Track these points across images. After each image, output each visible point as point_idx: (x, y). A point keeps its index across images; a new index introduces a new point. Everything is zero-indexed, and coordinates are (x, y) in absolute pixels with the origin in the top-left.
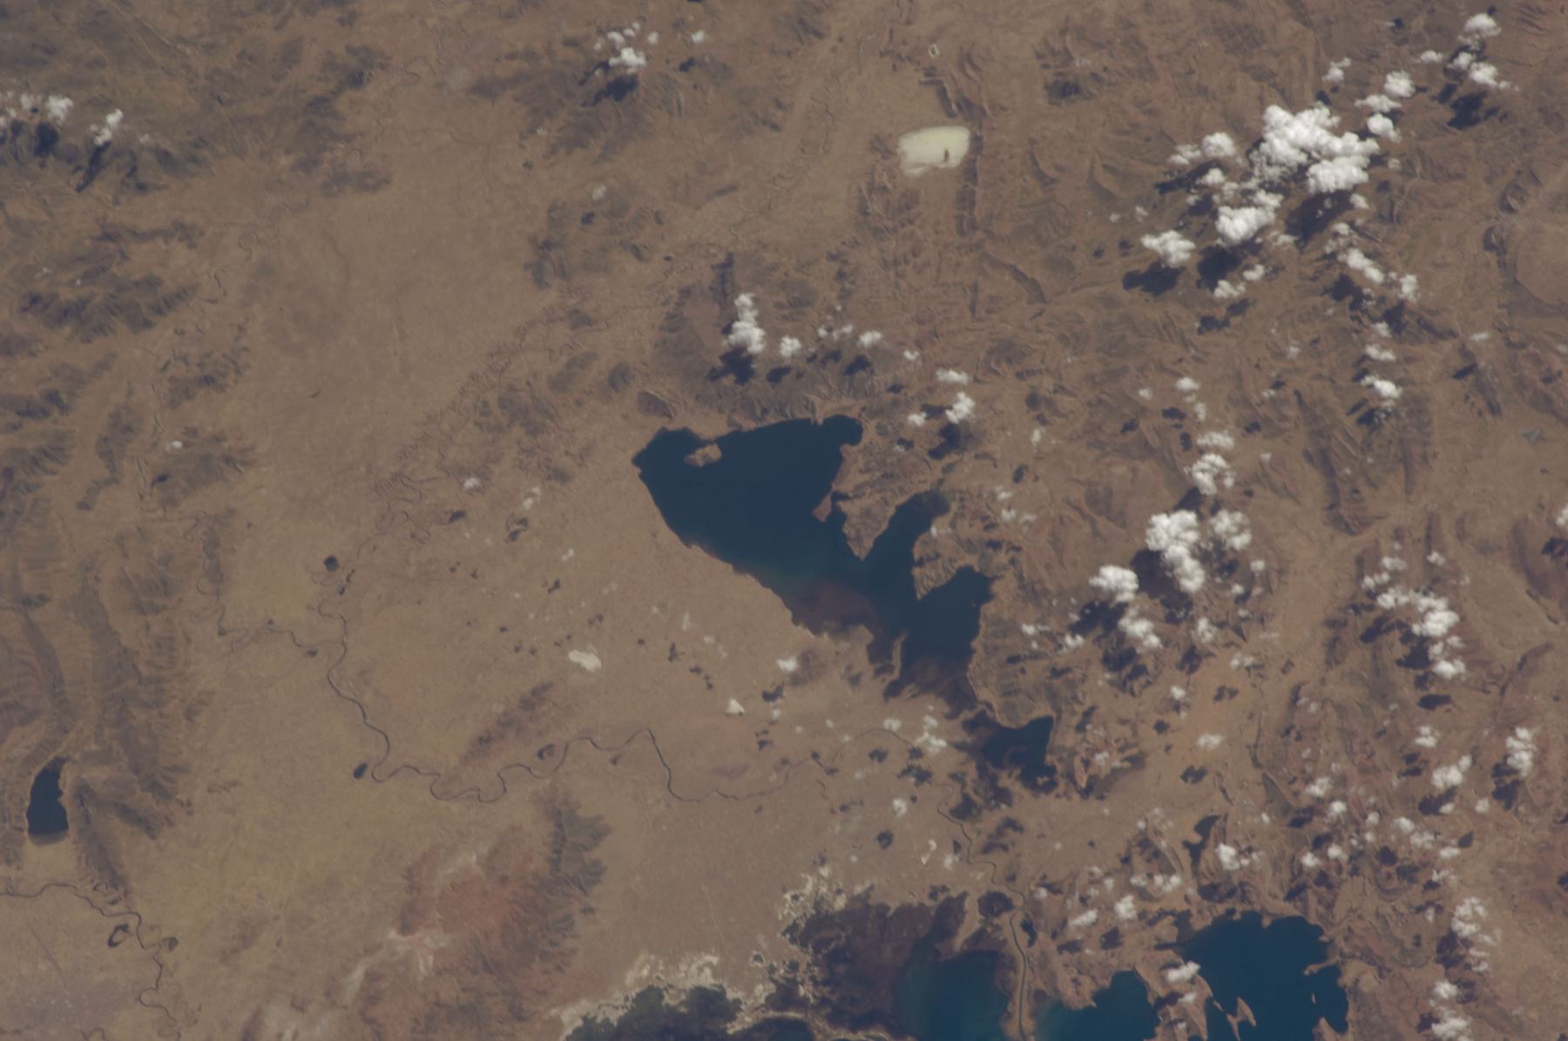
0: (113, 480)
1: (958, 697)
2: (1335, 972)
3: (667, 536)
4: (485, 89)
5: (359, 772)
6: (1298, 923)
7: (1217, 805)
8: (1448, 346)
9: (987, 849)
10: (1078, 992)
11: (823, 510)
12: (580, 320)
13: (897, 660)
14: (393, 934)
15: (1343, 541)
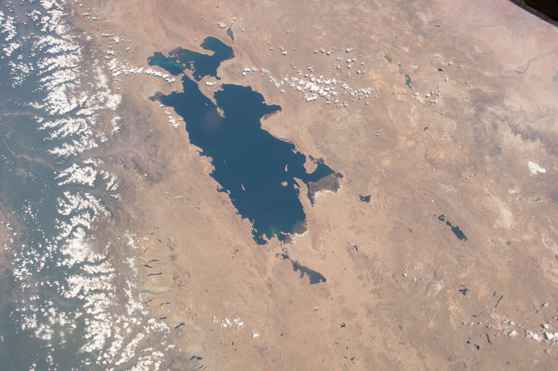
0: (366, 276)
1: (291, 261)
2: (255, 241)
3: (320, 273)
4: (356, 314)
5: (334, 252)
6: (260, 244)
7: (269, 253)
8: (268, 293)
9: (284, 249)
10: (272, 238)
11: (309, 276)
12: (337, 292)
13: (298, 264)
14: (324, 239)
15: (269, 276)
